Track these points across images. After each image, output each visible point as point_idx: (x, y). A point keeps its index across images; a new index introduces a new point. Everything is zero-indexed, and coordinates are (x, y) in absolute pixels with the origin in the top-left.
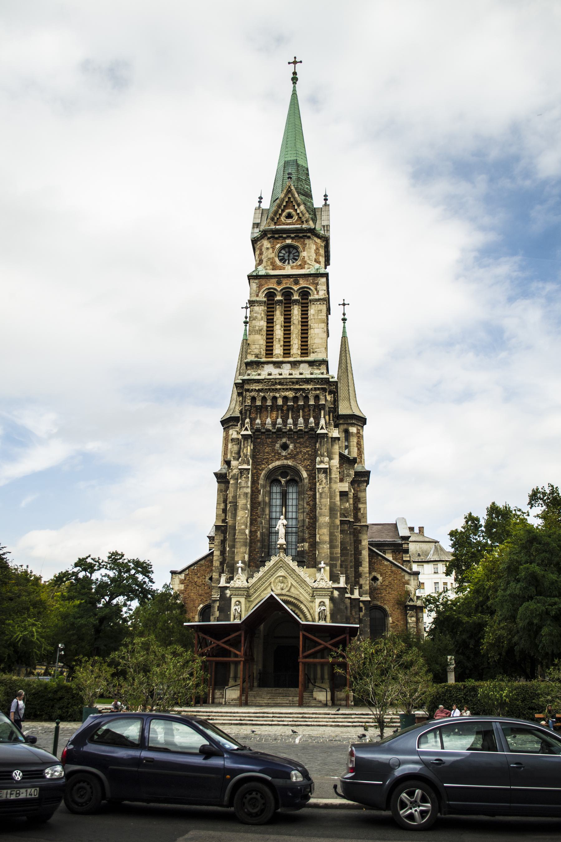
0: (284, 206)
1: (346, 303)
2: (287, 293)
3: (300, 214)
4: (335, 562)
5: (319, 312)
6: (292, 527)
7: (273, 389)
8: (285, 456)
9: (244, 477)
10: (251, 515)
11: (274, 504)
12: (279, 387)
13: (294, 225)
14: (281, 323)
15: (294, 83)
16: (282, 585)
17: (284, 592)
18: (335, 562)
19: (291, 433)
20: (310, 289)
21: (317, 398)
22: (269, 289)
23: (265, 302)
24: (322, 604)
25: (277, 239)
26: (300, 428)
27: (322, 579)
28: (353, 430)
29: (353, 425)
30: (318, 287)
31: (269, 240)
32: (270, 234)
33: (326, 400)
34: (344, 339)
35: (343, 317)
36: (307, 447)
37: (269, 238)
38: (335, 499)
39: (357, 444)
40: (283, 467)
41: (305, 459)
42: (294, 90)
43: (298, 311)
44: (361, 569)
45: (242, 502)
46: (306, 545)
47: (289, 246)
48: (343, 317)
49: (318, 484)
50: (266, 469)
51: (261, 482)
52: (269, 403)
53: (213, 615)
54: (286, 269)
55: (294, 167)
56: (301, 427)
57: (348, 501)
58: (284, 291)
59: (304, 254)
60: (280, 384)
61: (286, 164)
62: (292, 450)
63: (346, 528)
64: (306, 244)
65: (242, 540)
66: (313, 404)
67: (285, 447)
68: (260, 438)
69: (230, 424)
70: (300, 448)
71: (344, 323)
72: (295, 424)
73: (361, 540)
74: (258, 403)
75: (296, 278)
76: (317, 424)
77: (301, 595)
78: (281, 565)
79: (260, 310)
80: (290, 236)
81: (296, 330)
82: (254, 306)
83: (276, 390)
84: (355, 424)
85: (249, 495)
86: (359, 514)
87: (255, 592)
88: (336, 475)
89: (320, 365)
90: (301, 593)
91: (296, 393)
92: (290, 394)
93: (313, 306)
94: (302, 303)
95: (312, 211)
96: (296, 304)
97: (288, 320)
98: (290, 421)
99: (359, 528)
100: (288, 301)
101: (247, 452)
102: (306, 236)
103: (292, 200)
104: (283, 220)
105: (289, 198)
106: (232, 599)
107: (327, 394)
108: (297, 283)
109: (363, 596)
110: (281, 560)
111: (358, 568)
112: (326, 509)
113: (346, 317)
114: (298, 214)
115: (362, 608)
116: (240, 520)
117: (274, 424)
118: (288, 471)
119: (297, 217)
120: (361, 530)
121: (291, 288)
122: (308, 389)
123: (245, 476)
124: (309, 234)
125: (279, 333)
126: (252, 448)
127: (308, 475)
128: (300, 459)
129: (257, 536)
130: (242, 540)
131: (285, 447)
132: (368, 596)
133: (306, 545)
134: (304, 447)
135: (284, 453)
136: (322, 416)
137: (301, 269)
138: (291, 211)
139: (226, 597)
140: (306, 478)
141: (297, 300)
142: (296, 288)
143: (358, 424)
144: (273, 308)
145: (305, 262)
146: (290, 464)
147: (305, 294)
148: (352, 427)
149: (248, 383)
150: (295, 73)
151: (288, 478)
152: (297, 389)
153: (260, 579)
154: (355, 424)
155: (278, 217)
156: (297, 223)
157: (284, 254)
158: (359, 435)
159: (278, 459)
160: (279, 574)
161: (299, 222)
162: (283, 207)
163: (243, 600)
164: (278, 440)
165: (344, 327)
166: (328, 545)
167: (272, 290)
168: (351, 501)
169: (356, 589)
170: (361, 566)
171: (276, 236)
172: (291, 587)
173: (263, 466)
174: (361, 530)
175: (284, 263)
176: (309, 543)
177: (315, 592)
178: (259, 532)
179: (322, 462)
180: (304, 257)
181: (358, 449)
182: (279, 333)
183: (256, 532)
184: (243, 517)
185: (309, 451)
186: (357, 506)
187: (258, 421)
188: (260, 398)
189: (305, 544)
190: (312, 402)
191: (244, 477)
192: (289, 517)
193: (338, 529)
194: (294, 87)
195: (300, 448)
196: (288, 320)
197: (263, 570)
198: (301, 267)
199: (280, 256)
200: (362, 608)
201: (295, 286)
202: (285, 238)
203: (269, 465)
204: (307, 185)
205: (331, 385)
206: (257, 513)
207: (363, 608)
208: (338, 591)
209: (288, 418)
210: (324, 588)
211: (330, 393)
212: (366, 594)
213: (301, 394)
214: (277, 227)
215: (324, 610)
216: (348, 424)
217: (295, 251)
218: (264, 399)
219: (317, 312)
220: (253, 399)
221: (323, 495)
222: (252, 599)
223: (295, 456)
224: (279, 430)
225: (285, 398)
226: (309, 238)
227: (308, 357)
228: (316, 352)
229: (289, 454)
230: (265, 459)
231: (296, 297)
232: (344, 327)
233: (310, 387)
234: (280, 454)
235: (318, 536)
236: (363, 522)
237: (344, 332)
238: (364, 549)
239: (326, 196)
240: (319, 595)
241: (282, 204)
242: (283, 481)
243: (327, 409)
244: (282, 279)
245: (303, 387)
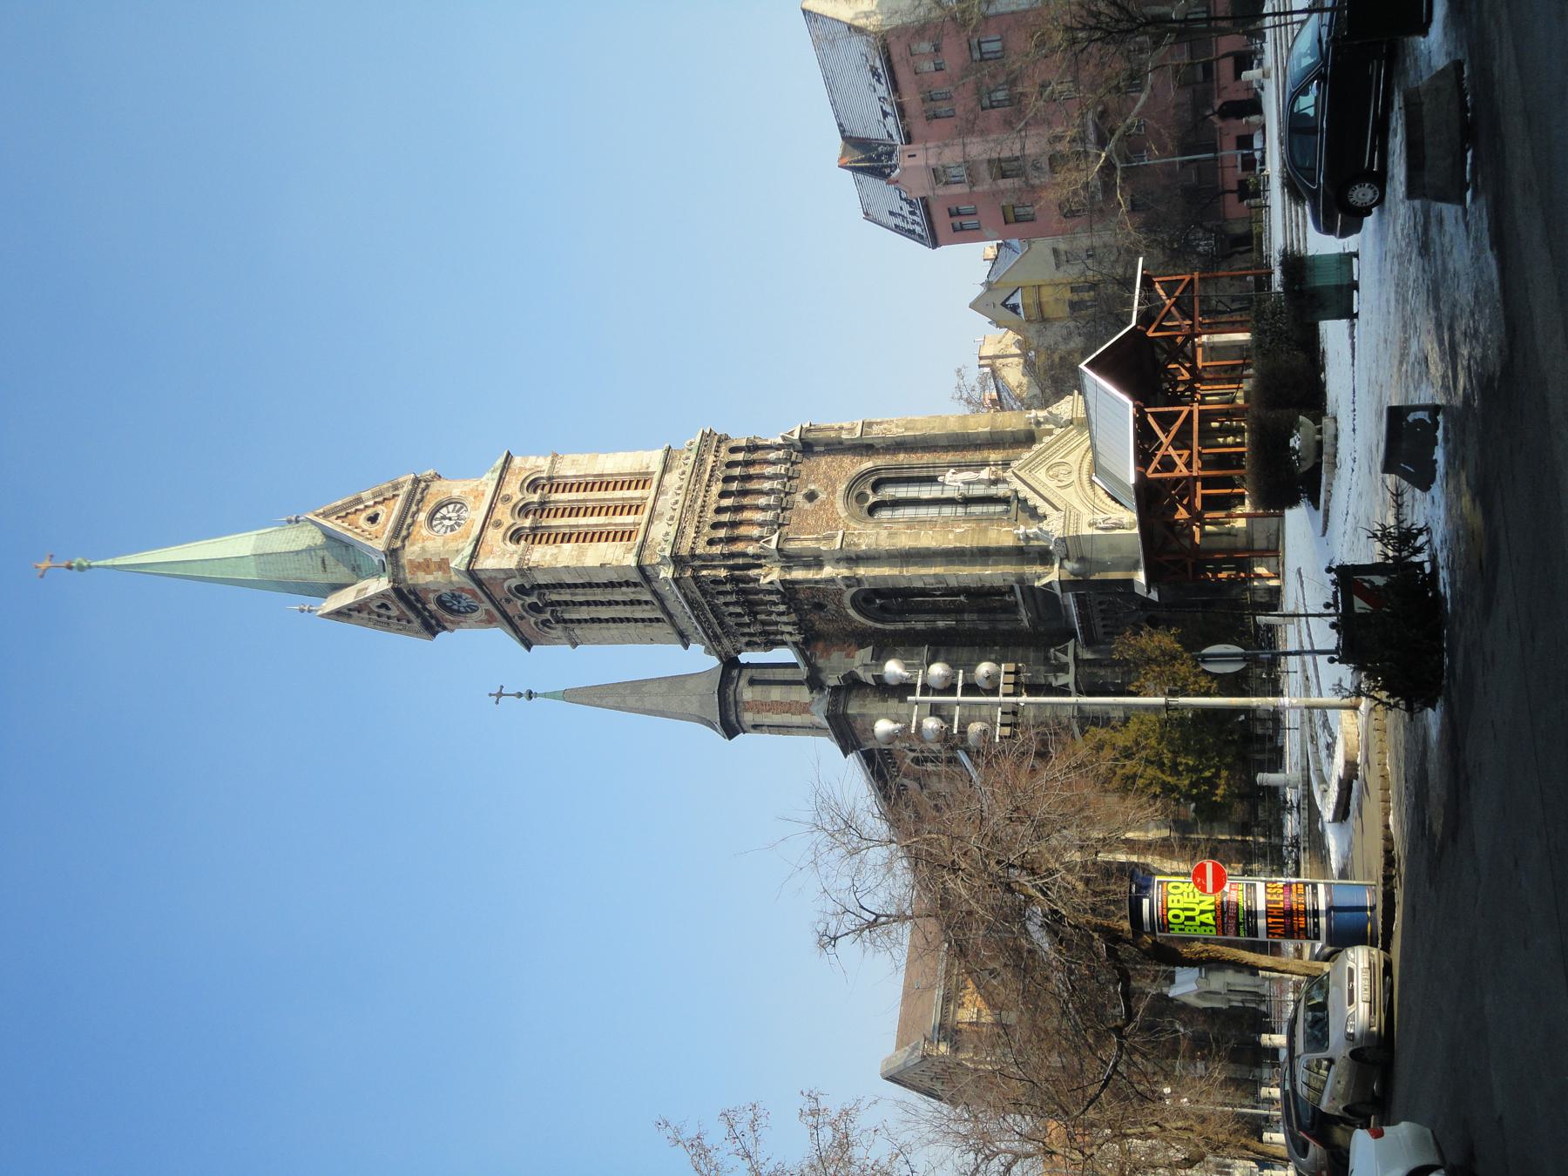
2: (524, 510)
7: (701, 512)
12: (699, 502)
17: (1076, 468)
22: (504, 539)
36: (818, 464)
41: (840, 466)
53: (1108, 713)
60: (694, 501)
65: (976, 536)
67: (811, 496)
69: (731, 699)
91: (718, 480)
92: (717, 488)
97: (574, 511)
102: (424, 490)
114: (376, 503)
116: (937, 541)
121: (515, 506)
123: (855, 539)
130: (976, 536)
135: (822, 496)
137: (483, 495)
139: (1080, 569)
145: (472, 490)
146: (844, 487)
152: (711, 476)
171: (404, 533)
202: (413, 523)
203: (840, 518)
221: (909, 426)
223: (831, 480)
225: (723, 495)
229: (826, 490)
230: (828, 523)
234: (823, 503)
242: (872, 499)
245: (709, 468)
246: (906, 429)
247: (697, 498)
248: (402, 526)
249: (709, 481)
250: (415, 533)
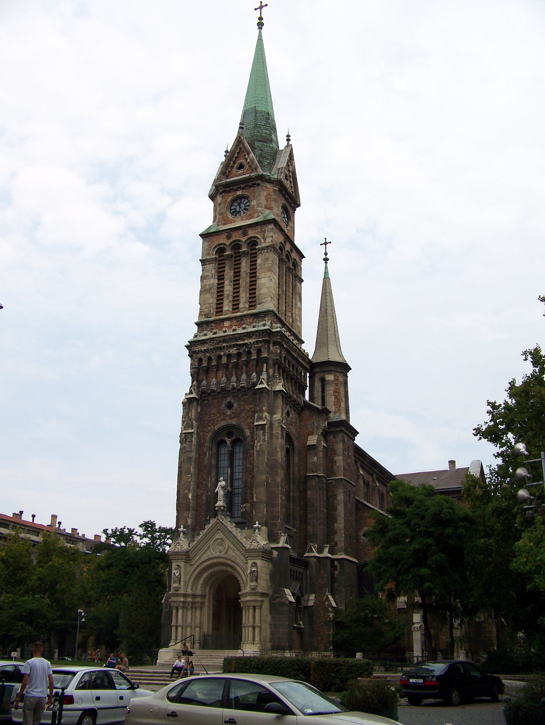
0: (235, 157)
1: (327, 241)
3: (250, 163)
4: (274, 522)
5: (266, 260)
6: (238, 488)
7: (217, 348)
8: (230, 415)
9: (188, 442)
10: (198, 479)
11: (222, 466)
13: (245, 174)
14: (231, 278)
15: (260, 28)
16: (220, 547)
17: (221, 555)
18: (274, 522)
19: (234, 391)
20: (257, 238)
21: (259, 351)
23: (216, 259)
24: (255, 564)
25: (228, 192)
26: (242, 385)
27: (254, 540)
28: (330, 377)
29: (329, 372)
30: (265, 234)
31: (222, 195)
32: (221, 189)
33: (269, 352)
34: (326, 280)
35: (324, 256)
36: (250, 404)
37: (221, 193)
38: (276, 456)
39: (335, 391)
40: (228, 427)
41: (248, 417)
42: (260, 36)
43: (246, 262)
44: (336, 525)
45: (186, 466)
46: (248, 505)
47: (241, 197)
48: (324, 256)
49: (256, 441)
50: (212, 430)
51: (207, 444)
52: (214, 363)
54: (237, 221)
55: (252, 115)
56: (243, 384)
57: (316, 455)
58: (233, 244)
59: (254, 203)
60: (224, 341)
62: (236, 409)
63: (314, 484)
64: (256, 192)
66: (255, 359)
67: (230, 406)
68: (206, 400)
70: (244, 405)
71: (326, 263)
72: (238, 380)
73: (336, 495)
74: (205, 364)
75: (243, 229)
76: (258, 378)
77: (237, 557)
78: (218, 528)
79: (212, 268)
80: (240, 187)
81: (244, 281)
82: (206, 264)
83: (221, 349)
84: (332, 371)
85: (193, 459)
86: (335, 467)
87: (195, 556)
88: (277, 430)
89: (265, 316)
90: (237, 555)
92: (234, 351)
93: (260, 255)
94: (251, 254)
95: (270, 155)
96: (244, 256)
97: (237, 274)
98: (234, 378)
99: (334, 482)
100: (237, 256)
101: (191, 416)
102: (255, 184)
103: (243, 149)
105: (241, 148)
106: (173, 563)
107: (271, 345)
108: (245, 234)
109: (338, 554)
110: (218, 523)
111: (334, 525)
112: (263, 467)
113: (328, 256)
115: (337, 566)
117: (218, 383)
118: (234, 431)
119: (248, 166)
120: (336, 484)
121: (239, 241)
122: (250, 343)
123: (189, 440)
124: (258, 182)
125: (228, 288)
126: (199, 410)
127: (250, 433)
128: (244, 417)
129: (203, 500)
131: (230, 406)
132: (343, 553)
133: (248, 505)
134: (247, 405)
135: (229, 412)
136: (265, 370)
138: (243, 161)
140: (249, 436)
141: (245, 251)
142: (243, 239)
143: (336, 370)
144: (224, 263)
146: (234, 423)
147: (253, 243)
148: (329, 374)
149: (195, 345)
150: (261, 18)
151: (233, 438)
152: (240, 344)
153: (199, 542)
154: (332, 371)
155: (229, 170)
156: (247, 173)
157: (236, 206)
158: (336, 382)
159: (223, 420)
160: (217, 537)
161: (250, 171)
162: (234, 159)
163: (182, 564)
164: (224, 400)
165: (326, 268)
166: (265, 505)
167: (222, 246)
168: (321, 454)
169: (326, 547)
170: (336, 522)
171: (227, 189)
172: (228, 550)
173: (209, 428)
174: (336, 484)
175: (236, 215)
176: (251, 503)
177: (249, 553)
178: (204, 496)
179: (260, 418)
180: (254, 205)
181: (336, 397)
182: (228, 288)
183: (202, 495)
184: (186, 481)
185: (252, 408)
186: (333, 459)
187: (204, 383)
188: (206, 359)
189: (247, 504)
190: (254, 357)
191: (188, 442)
192: (236, 478)
193: (278, 487)
194: (260, 32)
195: (244, 405)
196: (237, 274)
197: (202, 533)
198: (251, 217)
199: (233, 209)
200: (337, 566)
201: (244, 237)
202: (236, 190)
203: (214, 426)
204: (266, 130)
205: (274, 336)
206: (202, 476)
207: (338, 566)
208: (277, 551)
209: (232, 376)
210: (256, 549)
211: (275, 344)
212: (341, 551)
213: (244, 349)
214: (228, 180)
215: (254, 571)
216: (323, 371)
217: (246, 201)
218: (210, 359)
219: (264, 260)
220: (200, 360)
222: (193, 563)
223: (239, 414)
224: (223, 389)
225: (229, 356)
226: (258, 185)
227: (255, 309)
228: (262, 303)
229: (233, 413)
230: (212, 420)
231: (244, 249)
232: (326, 268)
233: (252, 341)
235: (255, 495)
236: (339, 476)
237: (326, 273)
238: (340, 504)
239: (288, 136)
240: (251, 557)
241: (233, 156)
243: (271, 362)
244: (231, 233)
245: (246, 342)
246: (258, 451)
247: (228, 342)
248: (231, 186)
249: (237, 345)
250: (229, 194)
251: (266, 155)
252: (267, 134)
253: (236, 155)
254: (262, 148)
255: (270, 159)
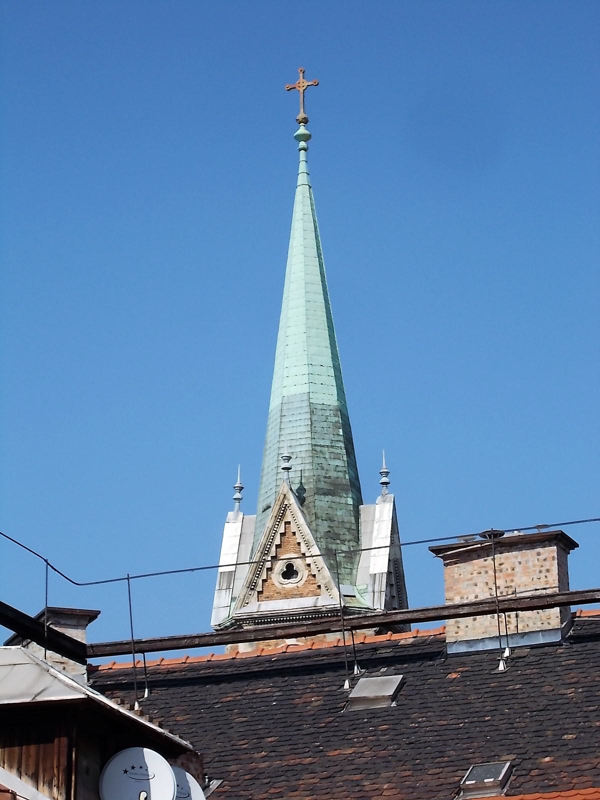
61: (285, 407)
95: (349, 529)
103: (293, 527)
104: (277, 584)
119: (306, 573)
155: (265, 578)
156: (307, 591)
251: (342, 531)
252: (338, 469)
253: (277, 541)
254: (330, 511)
255: (349, 541)
